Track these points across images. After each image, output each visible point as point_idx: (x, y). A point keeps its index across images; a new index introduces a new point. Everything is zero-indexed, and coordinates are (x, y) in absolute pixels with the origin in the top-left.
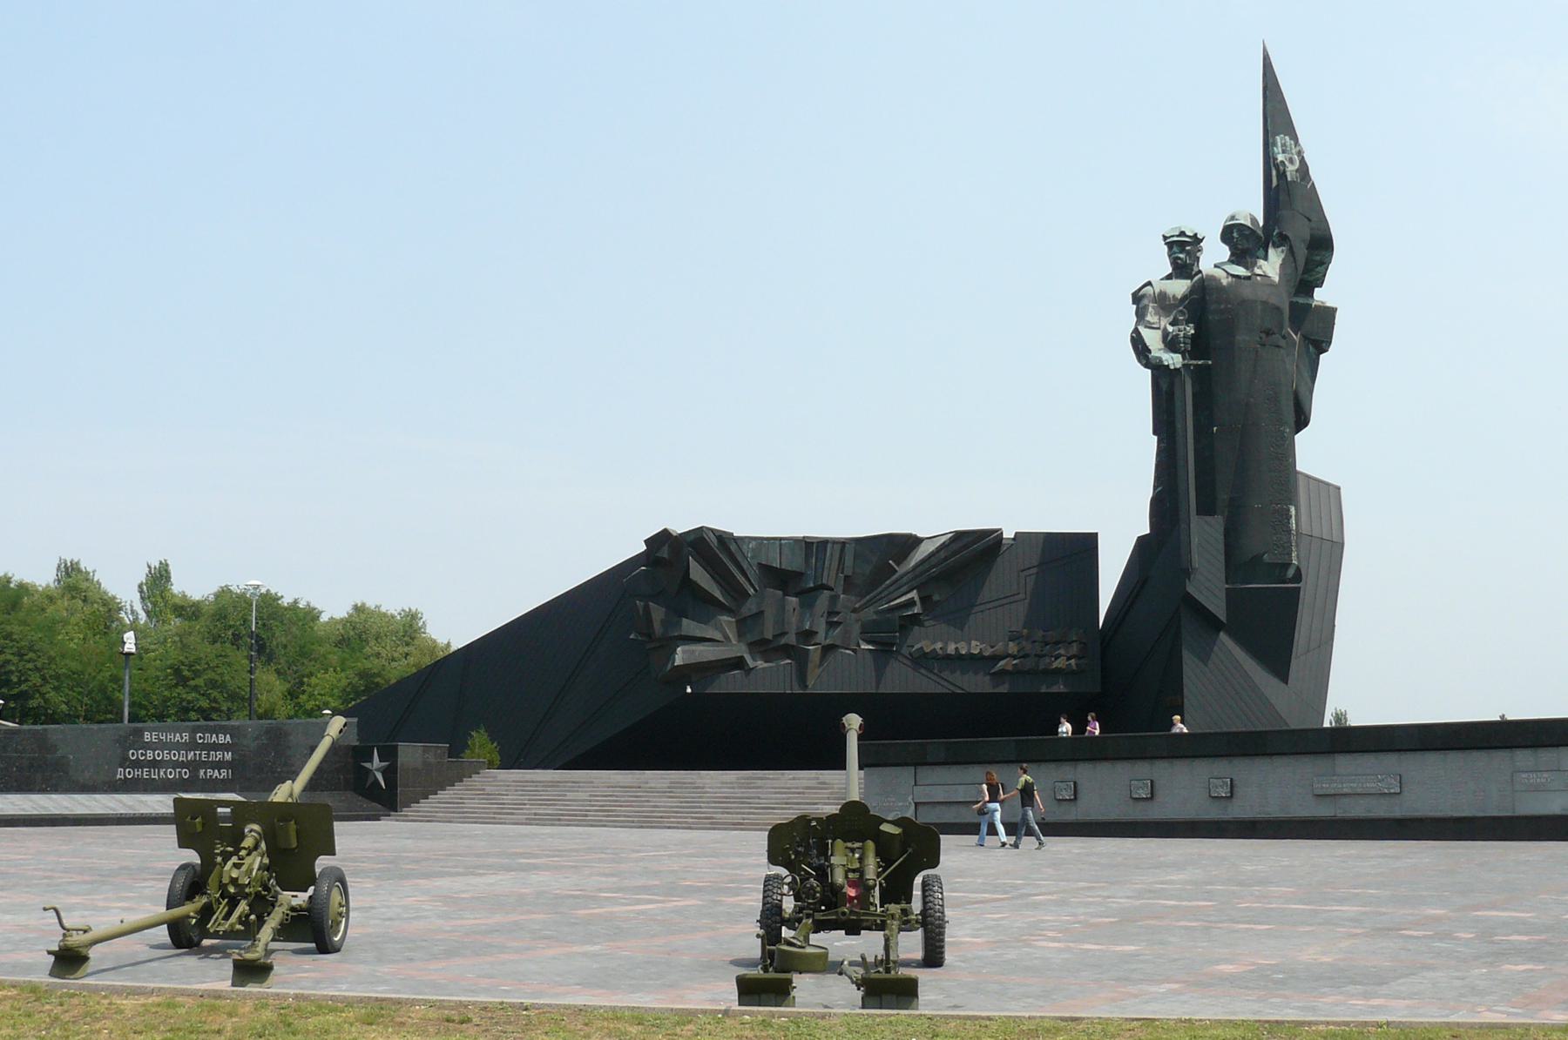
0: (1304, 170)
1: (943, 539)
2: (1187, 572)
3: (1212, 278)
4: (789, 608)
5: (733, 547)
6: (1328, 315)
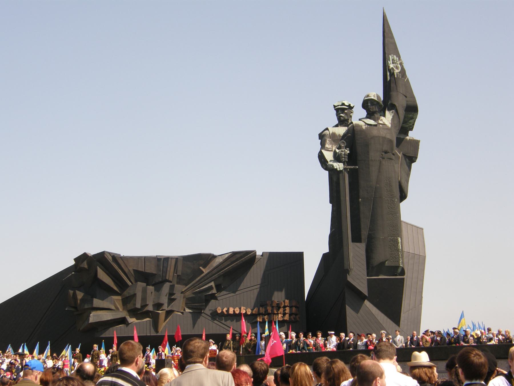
0: (403, 72)
1: (227, 256)
2: (347, 271)
3: (358, 125)
4: (149, 292)
5: (120, 262)
6: (416, 144)
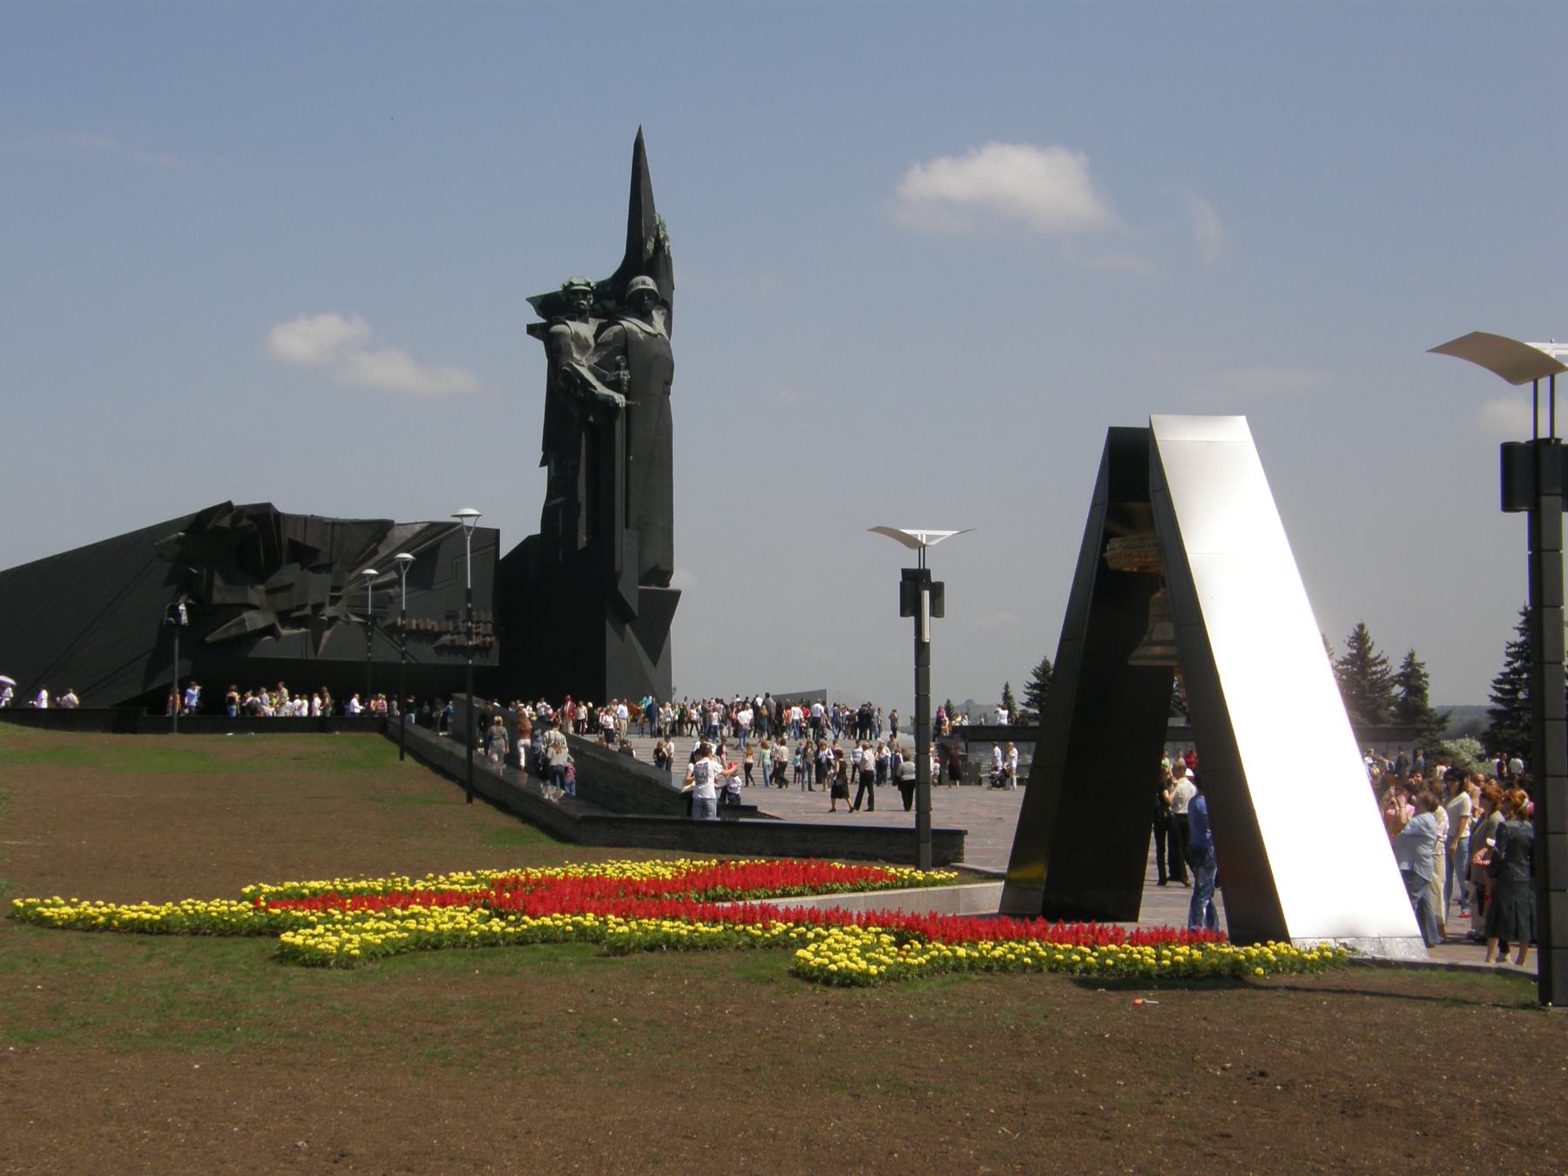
1: (418, 528)
